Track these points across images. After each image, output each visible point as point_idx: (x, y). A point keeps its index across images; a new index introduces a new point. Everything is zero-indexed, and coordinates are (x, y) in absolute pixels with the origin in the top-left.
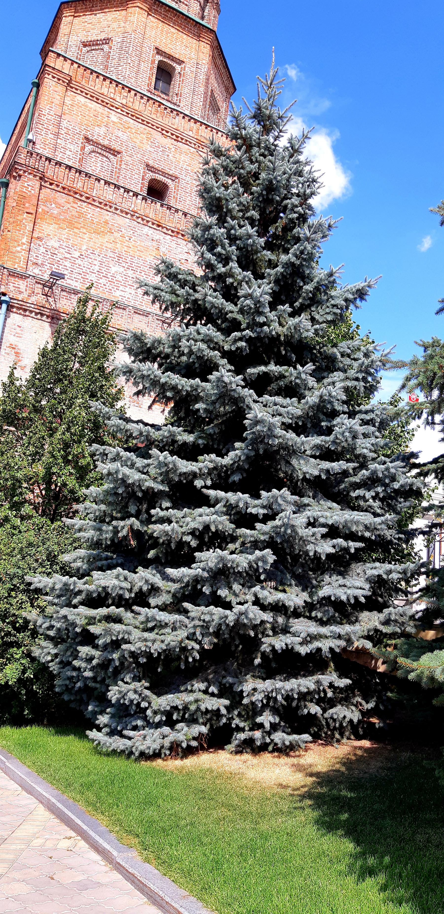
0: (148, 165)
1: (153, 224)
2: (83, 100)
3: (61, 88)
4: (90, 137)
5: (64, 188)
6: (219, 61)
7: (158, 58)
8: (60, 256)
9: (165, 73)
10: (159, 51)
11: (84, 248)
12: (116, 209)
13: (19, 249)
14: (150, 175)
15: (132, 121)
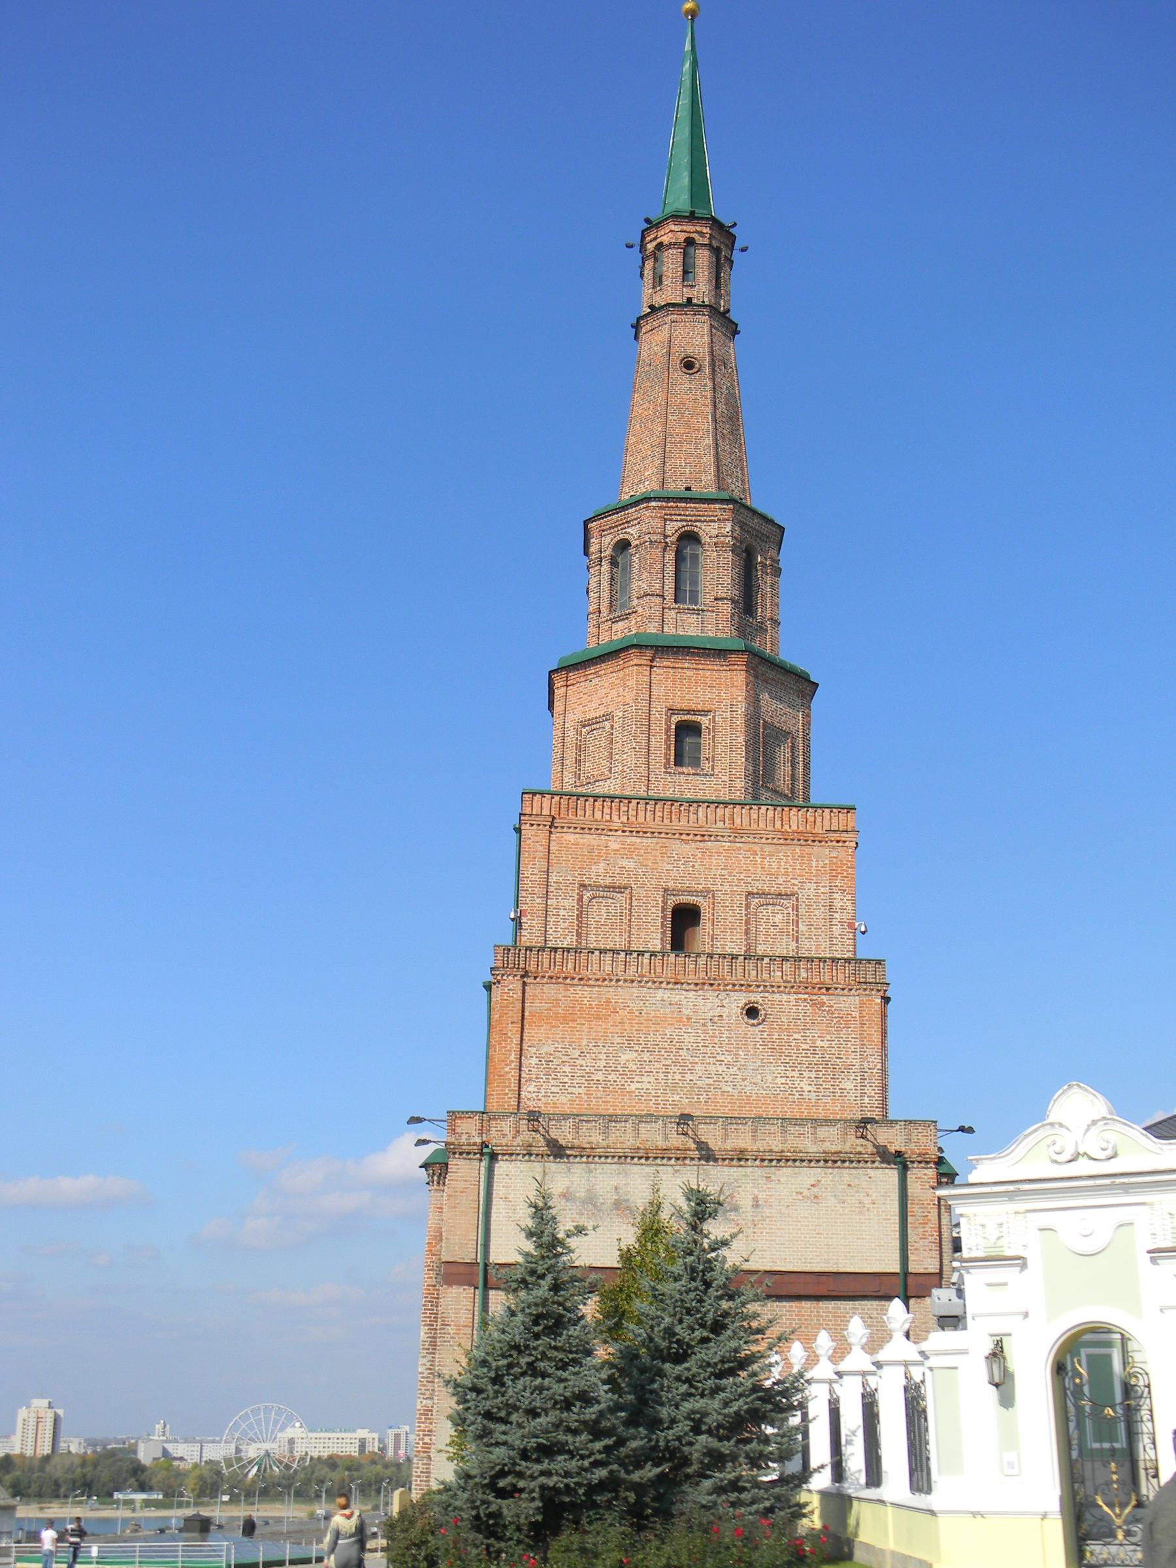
0: (666, 890)
1: (668, 983)
2: (571, 838)
3: (542, 836)
4: (587, 882)
5: (551, 978)
6: (771, 674)
7: (675, 719)
8: (556, 1061)
9: (686, 733)
10: (672, 711)
11: (584, 1043)
12: (618, 980)
13: (507, 1069)
14: (672, 901)
15: (639, 840)
